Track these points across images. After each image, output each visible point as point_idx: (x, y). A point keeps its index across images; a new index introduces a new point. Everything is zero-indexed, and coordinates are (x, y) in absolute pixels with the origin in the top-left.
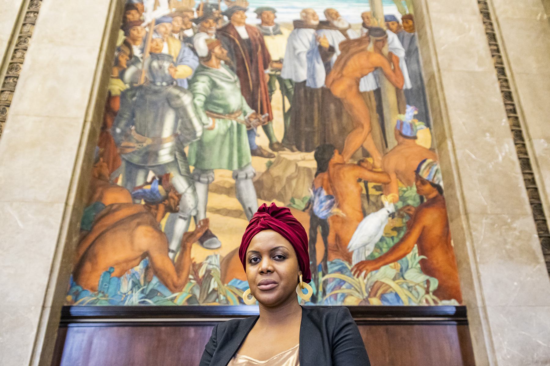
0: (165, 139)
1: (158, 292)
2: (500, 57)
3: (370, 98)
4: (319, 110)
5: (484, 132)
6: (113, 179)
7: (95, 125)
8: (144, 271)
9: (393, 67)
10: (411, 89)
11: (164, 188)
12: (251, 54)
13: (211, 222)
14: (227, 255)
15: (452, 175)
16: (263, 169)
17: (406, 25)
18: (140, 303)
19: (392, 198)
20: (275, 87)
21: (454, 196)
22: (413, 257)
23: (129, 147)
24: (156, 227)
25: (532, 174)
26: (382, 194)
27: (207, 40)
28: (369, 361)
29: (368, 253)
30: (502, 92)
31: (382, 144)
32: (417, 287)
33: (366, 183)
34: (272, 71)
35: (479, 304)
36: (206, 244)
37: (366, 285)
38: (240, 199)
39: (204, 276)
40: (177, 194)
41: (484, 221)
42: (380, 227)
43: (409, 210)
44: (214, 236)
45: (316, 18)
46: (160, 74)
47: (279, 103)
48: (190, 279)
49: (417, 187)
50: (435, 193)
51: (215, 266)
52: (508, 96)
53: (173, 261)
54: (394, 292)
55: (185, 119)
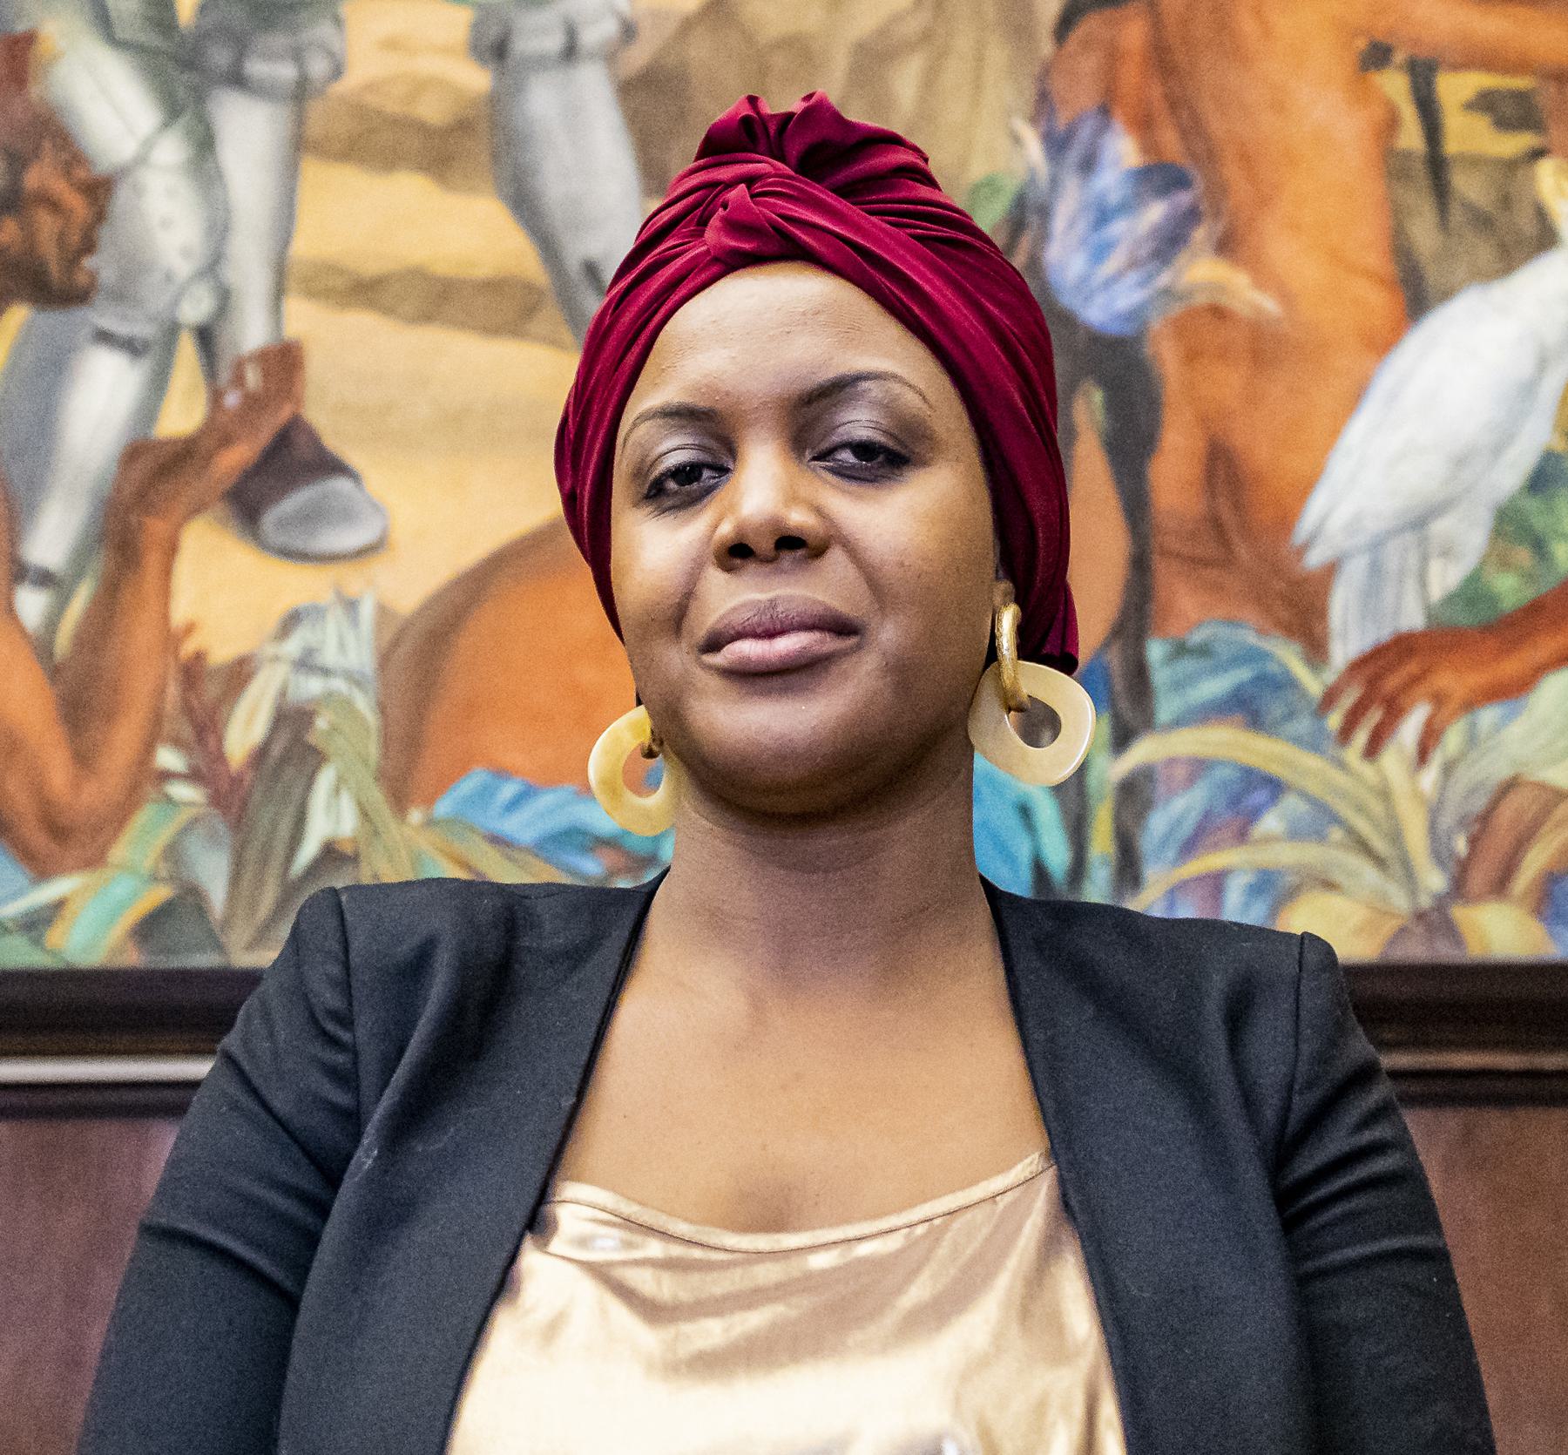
13: (317, 369)
29: (1445, 578)
36: (282, 524)
37: (1434, 814)
38: (524, 204)
39: (260, 754)
40: (81, 174)
42: (1528, 390)
48: (166, 776)
51: (339, 685)
53: (42, 647)
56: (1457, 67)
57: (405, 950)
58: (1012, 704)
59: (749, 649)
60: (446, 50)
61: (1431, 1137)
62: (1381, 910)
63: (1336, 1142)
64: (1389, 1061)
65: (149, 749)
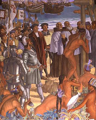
22: (84, 108)
24: (17, 101)
34: (47, 49)
38: (38, 93)
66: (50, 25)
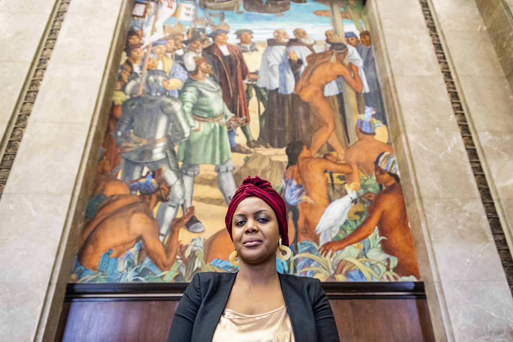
0: (158, 140)
1: (150, 270)
2: (446, 63)
3: (333, 101)
4: (289, 113)
5: (434, 127)
6: (114, 174)
7: (99, 129)
8: (138, 252)
9: (353, 75)
10: (369, 93)
11: (156, 181)
12: (232, 68)
14: (211, 237)
15: (407, 164)
16: (242, 163)
17: (364, 40)
18: (134, 280)
19: (354, 186)
20: (252, 94)
21: (409, 183)
22: (375, 238)
23: (127, 147)
24: (149, 213)
25: (479, 162)
26: (345, 183)
27: (194, 58)
28: (337, 332)
29: (334, 235)
30: (449, 92)
31: (345, 140)
32: (379, 265)
33: (331, 174)
34: (249, 81)
35: (435, 279)
37: (332, 264)
38: (221, 189)
39: (189, 256)
41: (437, 204)
42: (344, 212)
43: (369, 196)
44: (198, 221)
45: (286, 36)
46: (155, 86)
47: (255, 107)
48: (178, 259)
49: (376, 176)
50: (393, 181)
51: (199, 248)
52: (454, 96)
53: (163, 243)
54: (358, 269)
55: (176, 123)
56: (335, 173)
57: (207, 280)
58: (281, 250)
59: (249, 244)
60: (212, 171)
61: (332, 303)
62: (326, 276)
63: (320, 304)
64: (327, 294)
65: (176, 256)
66: (258, 34)
